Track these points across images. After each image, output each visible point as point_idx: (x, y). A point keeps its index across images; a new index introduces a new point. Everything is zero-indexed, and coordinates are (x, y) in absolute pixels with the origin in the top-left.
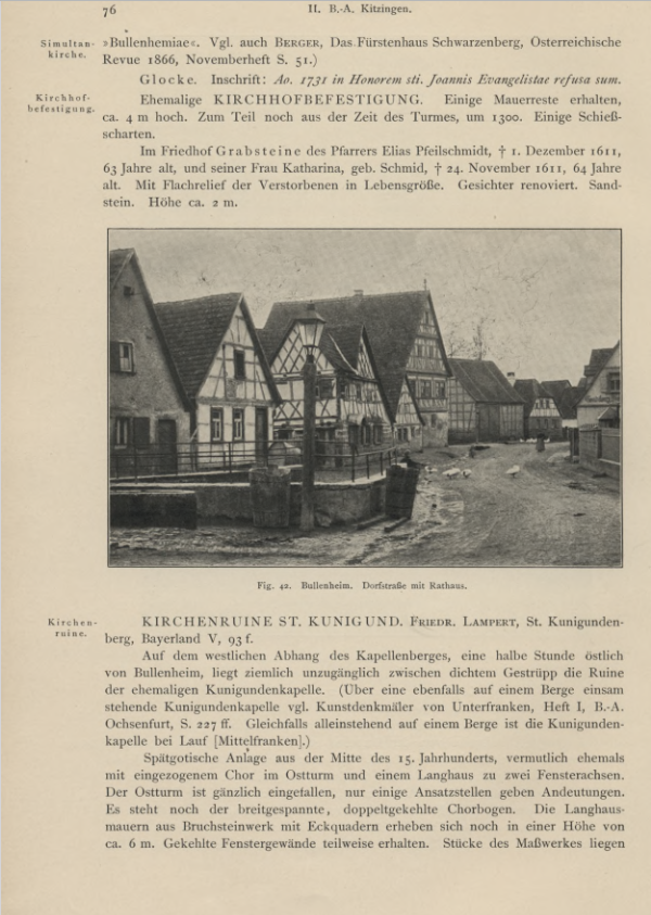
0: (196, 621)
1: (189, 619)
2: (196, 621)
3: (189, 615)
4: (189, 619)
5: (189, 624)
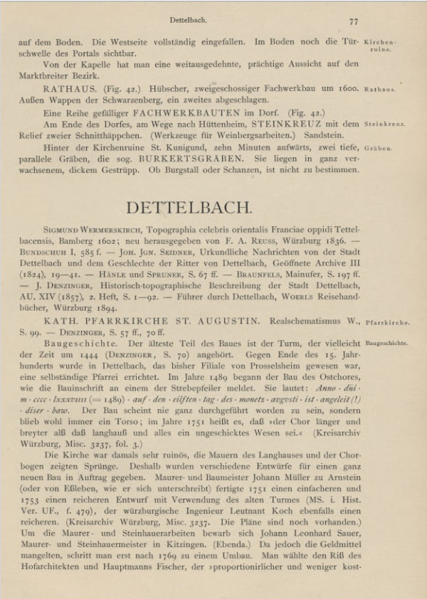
0: (161, 321)
1: (156, 319)
2: (161, 321)
3: (156, 317)
4: (156, 319)
5: (156, 322)
